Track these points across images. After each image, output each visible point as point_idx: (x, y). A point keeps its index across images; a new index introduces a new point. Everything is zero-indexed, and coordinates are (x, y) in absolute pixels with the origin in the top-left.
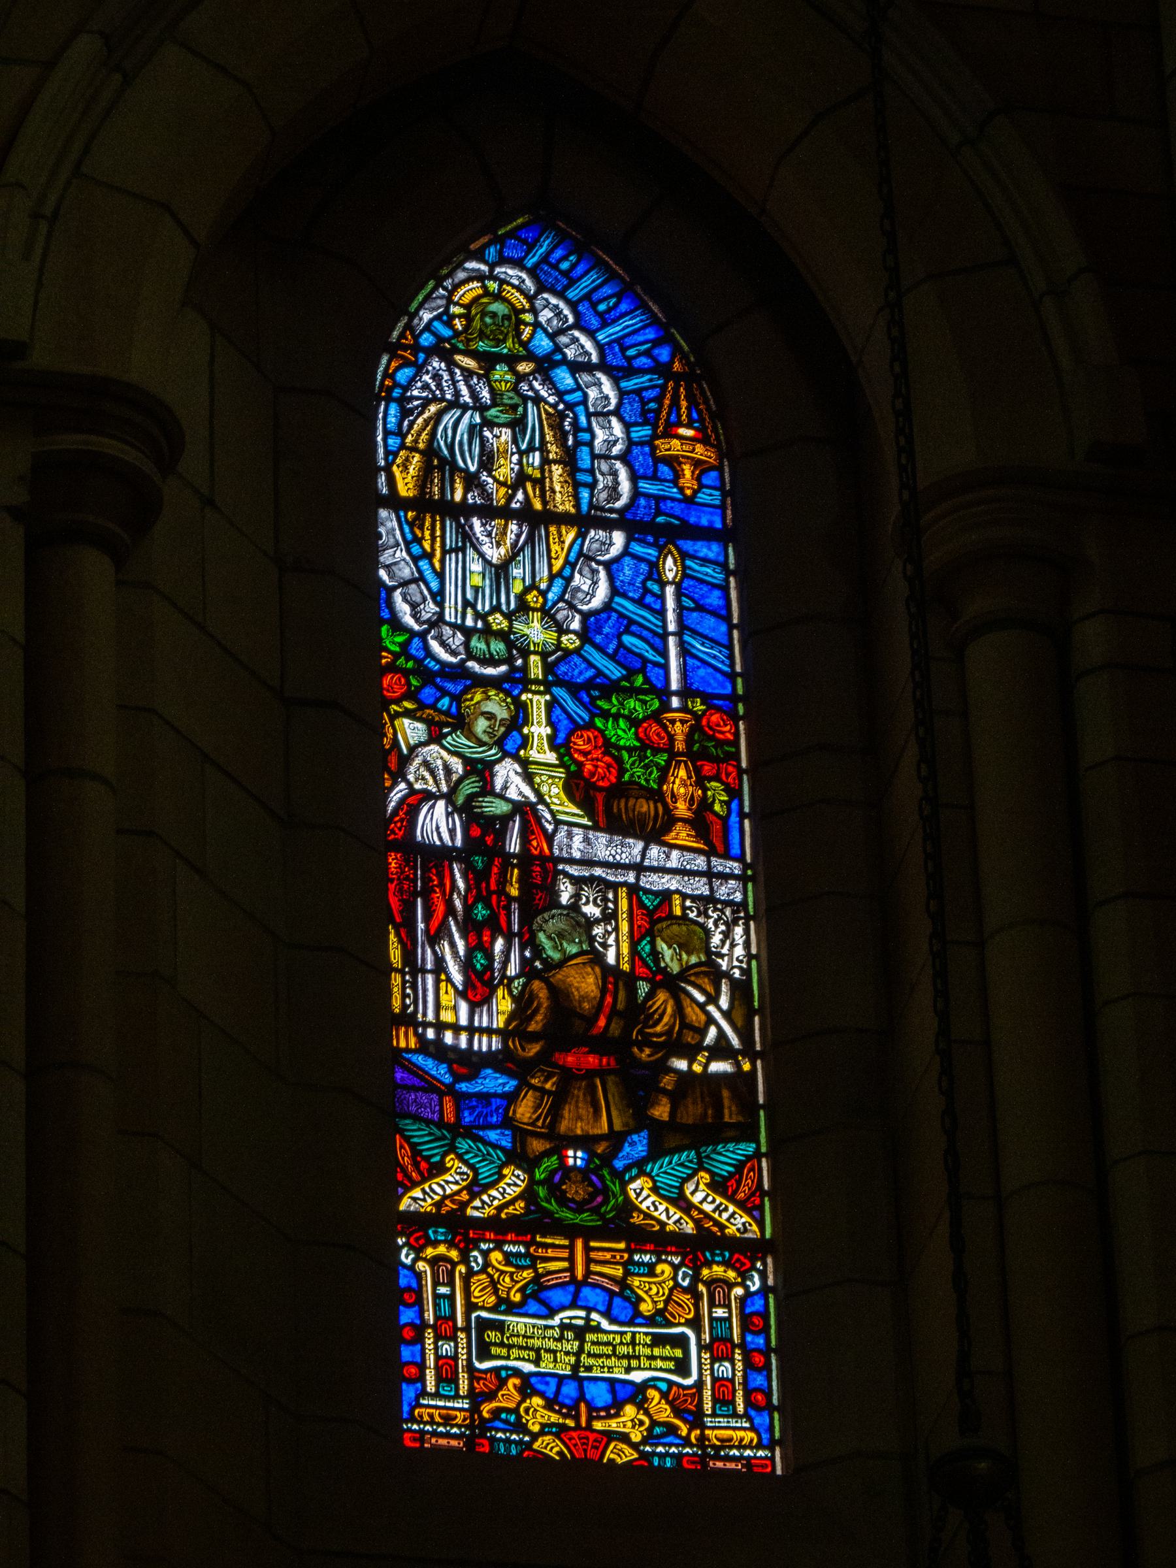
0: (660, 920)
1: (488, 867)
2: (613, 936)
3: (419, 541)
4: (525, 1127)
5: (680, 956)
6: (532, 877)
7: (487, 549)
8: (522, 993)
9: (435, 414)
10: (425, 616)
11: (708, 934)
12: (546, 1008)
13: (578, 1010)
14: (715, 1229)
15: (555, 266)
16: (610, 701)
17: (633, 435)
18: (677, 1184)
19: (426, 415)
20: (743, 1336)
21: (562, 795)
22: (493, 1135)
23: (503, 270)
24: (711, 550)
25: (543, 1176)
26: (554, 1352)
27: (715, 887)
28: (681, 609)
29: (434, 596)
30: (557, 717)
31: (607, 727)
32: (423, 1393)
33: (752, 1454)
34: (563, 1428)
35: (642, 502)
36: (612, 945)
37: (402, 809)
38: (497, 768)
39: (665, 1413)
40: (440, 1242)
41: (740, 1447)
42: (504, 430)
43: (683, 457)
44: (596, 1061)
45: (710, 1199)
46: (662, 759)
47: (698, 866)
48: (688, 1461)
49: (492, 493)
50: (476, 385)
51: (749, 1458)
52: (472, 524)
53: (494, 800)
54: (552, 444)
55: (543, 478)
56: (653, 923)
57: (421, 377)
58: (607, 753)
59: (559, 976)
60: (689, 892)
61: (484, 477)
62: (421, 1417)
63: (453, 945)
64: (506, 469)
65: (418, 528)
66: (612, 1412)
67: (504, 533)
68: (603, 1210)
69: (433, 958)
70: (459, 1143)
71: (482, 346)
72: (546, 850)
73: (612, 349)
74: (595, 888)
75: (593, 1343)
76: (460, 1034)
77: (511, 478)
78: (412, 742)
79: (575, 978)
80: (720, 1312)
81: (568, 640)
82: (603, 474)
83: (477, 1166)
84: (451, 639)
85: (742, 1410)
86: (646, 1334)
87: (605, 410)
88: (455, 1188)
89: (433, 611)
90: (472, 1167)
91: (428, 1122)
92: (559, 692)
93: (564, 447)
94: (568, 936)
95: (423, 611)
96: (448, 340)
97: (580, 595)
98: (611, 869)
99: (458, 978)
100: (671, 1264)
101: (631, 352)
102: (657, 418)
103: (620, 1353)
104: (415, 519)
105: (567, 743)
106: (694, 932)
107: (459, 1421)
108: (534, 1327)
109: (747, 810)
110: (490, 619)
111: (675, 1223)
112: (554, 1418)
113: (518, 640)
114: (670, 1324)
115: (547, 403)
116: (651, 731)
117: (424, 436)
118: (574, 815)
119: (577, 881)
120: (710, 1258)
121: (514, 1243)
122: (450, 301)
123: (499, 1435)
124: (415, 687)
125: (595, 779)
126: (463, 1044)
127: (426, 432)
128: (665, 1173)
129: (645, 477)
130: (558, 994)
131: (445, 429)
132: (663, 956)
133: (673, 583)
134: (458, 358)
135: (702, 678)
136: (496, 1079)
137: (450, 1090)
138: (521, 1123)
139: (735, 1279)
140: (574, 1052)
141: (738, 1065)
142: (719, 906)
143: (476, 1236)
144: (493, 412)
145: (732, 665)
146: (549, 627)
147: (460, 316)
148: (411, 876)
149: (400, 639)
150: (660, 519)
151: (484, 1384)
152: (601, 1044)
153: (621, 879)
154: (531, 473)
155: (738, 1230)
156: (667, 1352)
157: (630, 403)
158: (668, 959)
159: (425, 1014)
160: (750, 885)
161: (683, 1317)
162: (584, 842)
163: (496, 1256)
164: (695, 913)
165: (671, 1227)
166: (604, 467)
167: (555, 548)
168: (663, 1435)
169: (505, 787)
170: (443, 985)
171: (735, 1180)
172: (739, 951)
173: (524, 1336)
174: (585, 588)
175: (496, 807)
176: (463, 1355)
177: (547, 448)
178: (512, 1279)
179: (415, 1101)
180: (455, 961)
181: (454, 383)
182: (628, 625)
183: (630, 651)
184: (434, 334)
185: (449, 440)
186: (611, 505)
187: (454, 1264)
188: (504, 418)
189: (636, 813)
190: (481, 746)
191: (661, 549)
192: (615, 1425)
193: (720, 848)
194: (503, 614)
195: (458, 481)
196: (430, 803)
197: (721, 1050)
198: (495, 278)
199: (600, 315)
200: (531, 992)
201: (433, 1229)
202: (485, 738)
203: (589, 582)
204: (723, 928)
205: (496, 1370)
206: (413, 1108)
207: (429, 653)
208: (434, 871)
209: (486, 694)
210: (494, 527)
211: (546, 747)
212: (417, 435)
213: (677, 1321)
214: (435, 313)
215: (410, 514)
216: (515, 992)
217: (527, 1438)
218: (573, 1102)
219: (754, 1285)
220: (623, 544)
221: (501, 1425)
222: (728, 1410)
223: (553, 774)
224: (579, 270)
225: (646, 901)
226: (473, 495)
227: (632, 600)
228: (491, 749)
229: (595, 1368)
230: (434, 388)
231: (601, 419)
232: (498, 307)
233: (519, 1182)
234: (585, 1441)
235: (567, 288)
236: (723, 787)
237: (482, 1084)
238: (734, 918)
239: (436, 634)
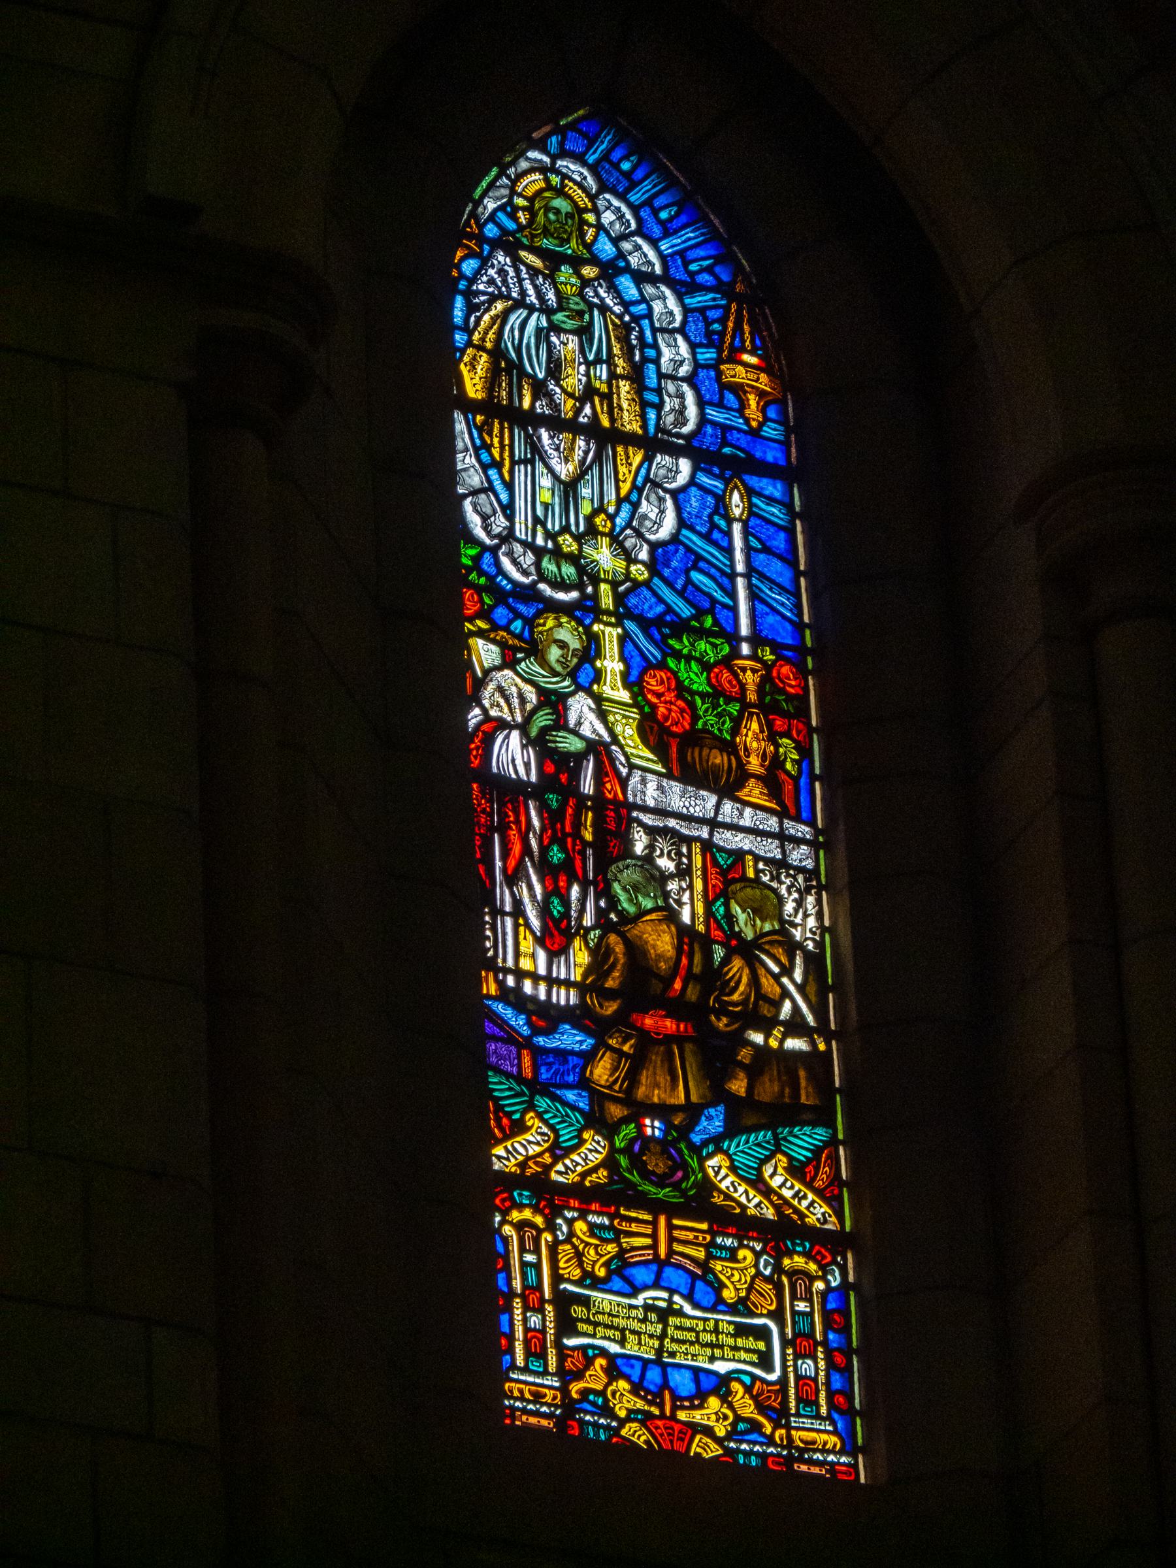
0: (734, 881)
1: (563, 805)
2: (687, 894)
3: (488, 447)
4: (602, 1089)
5: (754, 921)
6: (606, 823)
7: (554, 463)
8: (598, 945)
9: (502, 312)
10: (497, 530)
11: (781, 901)
12: (623, 964)
13: (655, 970)
14: (795, 1217)
15: (616, 166)
16: (681, 641)
17: (699, 357)
18: (756, 1166)
19: (493, 312)
20: (825, 1334)
21: (636, 737)
22: (570, 1096)
23: (565, 163)
24: (774, 489)
25: (622, 1145)
26: (639, 1334)
27: (788, 852)
28: (748, 550)
29: (504, 508)
30: (630, 653)
31: (680, 669)
32: (513, 1367)
33: (835, 1460)
34: (648, 1416)
35: (709, 429)
36: (686, 903)
37: (478, 736)
38: (570, 701)
39: (748, 1409)
40: (525, 1206)
41: (824, 1451)
42: (571, 337)
43: (748, 385)
44: (674, 1026)
45: (788, 1184)
46: (734, 709)
47: (771, 827)
48: (773, 1461)
49: (560, 403)
50: (542, 285)
51: (832, 1464)
52: (541, 435)
53: (568, 736)
54: (620, 358)
55: (611, 393)
56: (728, 883)
57: (487, 270)
58: (680, 696)
59: (634, 931)
60: (762, 853)
61: (552, 386)
62: (511, 1391)
63: (530, 887)
64: (574, 379)
65: (487, 434)
66: (696, 1402)
67: (572, 449)
68: (684, 1185)
69: (511, 900)
70: (537, 1101)
71: (546, 243)
72: (620, 796)
73: (675, 261)
74: (669, 840)
75: (677, 1328)
76: (539, 984)
77: (579, 390)
78: (486, 665)
79: (651, 935)
80: (802, 1306)
81: (637, 571)
82: (670, 396)
83: (558, 1127)
84: (522, 557)
85: (825, 1412)
86: (729, 1323)
87: (671, 327)
88: (538, 1149)
89: (503, 525)
90: (552, 1127)
91: (508, 1075)
92: (629, 624)
93: (630, 362)
94: (643, 890)
95: (493, 524)
96: (513, 233)
97: (648, 523)
98: (685, 821)
99: (536, 923)
100: (752, 1250)
101: (693, 267)
102: (722, 342)
103: (703, 1340)
104: (484, 423)
105: (640, 681)
106: (767, 897)
107: (548, 1399)
108: (618, 1305)
109: (817, 771)
110: (560, 539)
111: (756, 1206)
112: (640, 1404)
113: (588, 565)
114: (752, 1314)
115: (613, 313)
116: (722, 676)
117: (491, 335)
118: (648, 760)
119: (651, 831)
120: (790, 1247)
121: (599, 1213)
122: (513, 192)
123: (588, 1418)
124: (488, 605)
125: (668, 724)
126: (542, 996)
127: (493, 331)
128: (742, 1152)
129: (711, 404)
130: (636, 951)
131: (512, 330)
132: (737, 919)
133: (739, 520)
134: (522, 253)
135: (771, 625)
136: (575, 1035)
137: (528, 1043)
138: (600, 1086)
139: (816, 1272)
140: (652, 1015)
141: (813, 1044)
142: (792, 872)
143: (560, 1203)
144: (559, 317)
145: (800, 614)
146: (618, 554)
147: (524, 209)
148: (488, 809)
149: (473, 552)
150: (726, 450)
151: (572, 1362)
152: (676, 1008)
153: (696, 833)
154: (598, 387)
155: (818, 1220)
156: (750, 1343)
157: (694, 322)
158: (742, 923)
159: (504, 960)
160: (822, 853)
161: (766, 1308)
162: (657, 790)
163: (580, 1226)
164: (768, 878)
165: (751, 1211)
166: (671, 387)
167: (622, 469)
168: (747, 1432)
169: (579, 724)
170: (522, 929)
171: (813, 1166)
172: (812, 922)
173: (610, 1315)
174: (652, 516)
175: (570, 744)
176: (550, 1329)
177: (614, 361)
178: (597, 1253)
179: (495, 1052)
180: (533, 904)
181: (520, 281)
182: (696, 561)
183: (698, 589)
184: (498, 225)
185: (516, 342)
186: (678, 430)
187: (540, 1231)
188: (570, 324)
189: (710, 764)
190: (554, 676)
191: (727, 482)
192: (699, 1417)
193: (793, 811)
194: (572, 535)
195: (526, 387)
196: (505, 732)
197: (796, 1026)
198: (557, 172)
199: (661, 222)
200: (608, 945)
201: (518, 1191)
202: (558, 668)
203: (657, 511)
204: (796, 895)
205: (583, 1348)
206: (494, 1059)
207: (501, 571)
208: (510, 806)
209: (558, 620)
210: (562, 440)
211: (619, 684)
212: (484, 333)
213: (759, 1312)
214: (499, 203)
215: (479, 418)
216: (592, 944)
217: (614, 1424)
218: (651, 1069)
219: (835, 1280)
220: (689, 473)
221: (589, 1408)
222: (812, 1411)
223: (627, 713)
224: (639, 174)
225: (720, 859)
226: (542, 405)
227: (699, 533)
228: (564, 680)
229: (678, 1354)
230: (500, 284)
231: (666, 336)
232: (558, 203)
233: (600, 1149)
234: (671, 1431)
235: (629, 190)
236: (793, 745)
237: (561, 1040)
238: (807, 886)
239: (507, 551)
